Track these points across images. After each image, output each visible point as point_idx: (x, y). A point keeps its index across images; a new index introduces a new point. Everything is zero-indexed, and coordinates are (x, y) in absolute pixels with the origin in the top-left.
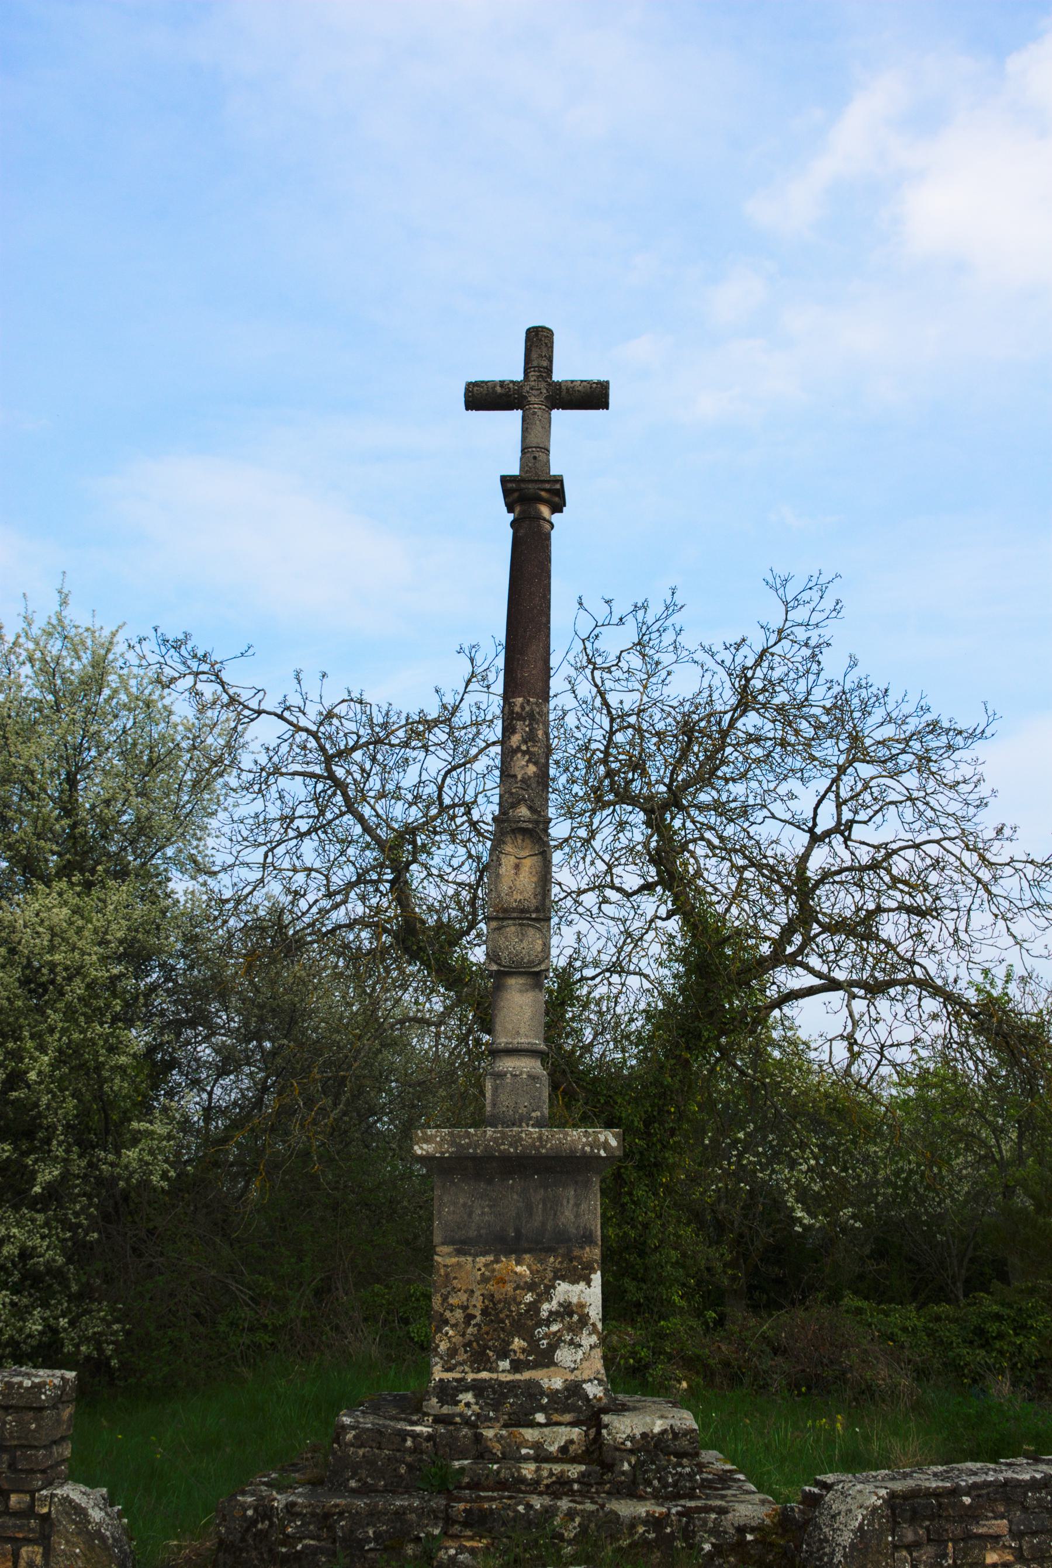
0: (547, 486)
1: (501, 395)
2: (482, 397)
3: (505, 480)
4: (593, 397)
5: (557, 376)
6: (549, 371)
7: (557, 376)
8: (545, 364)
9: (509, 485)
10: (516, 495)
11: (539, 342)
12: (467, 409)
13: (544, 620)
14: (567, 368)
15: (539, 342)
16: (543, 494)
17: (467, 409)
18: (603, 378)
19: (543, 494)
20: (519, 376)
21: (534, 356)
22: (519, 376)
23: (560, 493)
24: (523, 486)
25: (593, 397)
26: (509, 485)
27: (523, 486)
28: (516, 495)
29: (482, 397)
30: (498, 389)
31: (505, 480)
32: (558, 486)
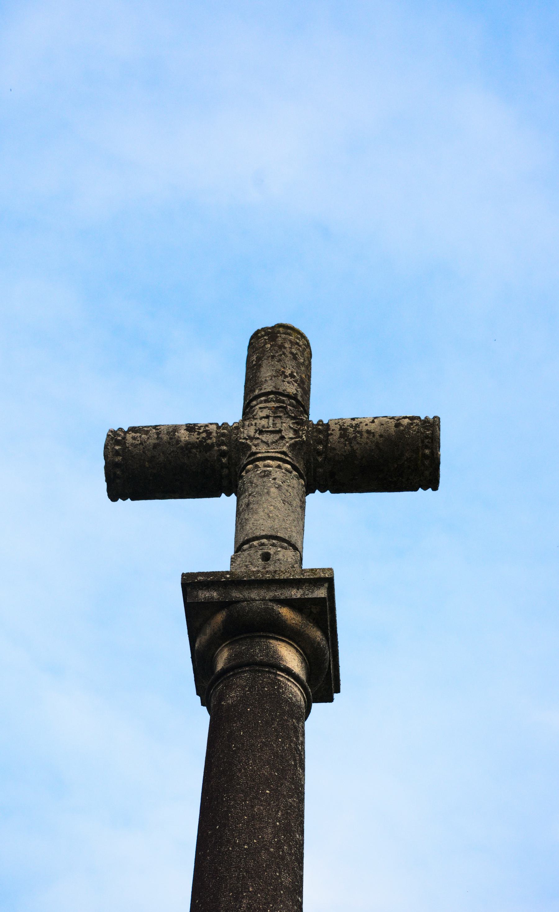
0: (296, 593)
1: (189, 446)
2: (145, 467)
3: (191, 584)
4: (402, 458)
5: (319, 411)
6: (301, 404)
7: (319, 411)
8: (292, 389)
9: (203, 595)
10: (220, 618)
11: (277, 353)
12: (115, 493)
13: (286, 880)
14: (341, 396)
15: (277, 353)
16: (285, 612)
17: (115, 493)
18: (425, 412)
19: (285, 612)
20: (230, 412)
21: (266, 372)
22: (230, 412)
23: (322, 613)
24: (236, 594)
25: (402, 458)
26: (203, 595)
27: (236, 594)
28: (220, 618)
29: (145, 467)
30: (183, 435)
31: (191, 584)
32: (321, 593)
